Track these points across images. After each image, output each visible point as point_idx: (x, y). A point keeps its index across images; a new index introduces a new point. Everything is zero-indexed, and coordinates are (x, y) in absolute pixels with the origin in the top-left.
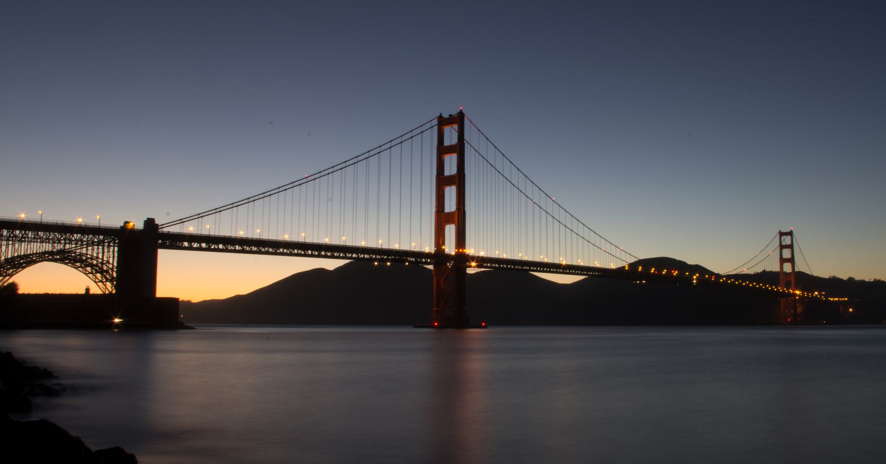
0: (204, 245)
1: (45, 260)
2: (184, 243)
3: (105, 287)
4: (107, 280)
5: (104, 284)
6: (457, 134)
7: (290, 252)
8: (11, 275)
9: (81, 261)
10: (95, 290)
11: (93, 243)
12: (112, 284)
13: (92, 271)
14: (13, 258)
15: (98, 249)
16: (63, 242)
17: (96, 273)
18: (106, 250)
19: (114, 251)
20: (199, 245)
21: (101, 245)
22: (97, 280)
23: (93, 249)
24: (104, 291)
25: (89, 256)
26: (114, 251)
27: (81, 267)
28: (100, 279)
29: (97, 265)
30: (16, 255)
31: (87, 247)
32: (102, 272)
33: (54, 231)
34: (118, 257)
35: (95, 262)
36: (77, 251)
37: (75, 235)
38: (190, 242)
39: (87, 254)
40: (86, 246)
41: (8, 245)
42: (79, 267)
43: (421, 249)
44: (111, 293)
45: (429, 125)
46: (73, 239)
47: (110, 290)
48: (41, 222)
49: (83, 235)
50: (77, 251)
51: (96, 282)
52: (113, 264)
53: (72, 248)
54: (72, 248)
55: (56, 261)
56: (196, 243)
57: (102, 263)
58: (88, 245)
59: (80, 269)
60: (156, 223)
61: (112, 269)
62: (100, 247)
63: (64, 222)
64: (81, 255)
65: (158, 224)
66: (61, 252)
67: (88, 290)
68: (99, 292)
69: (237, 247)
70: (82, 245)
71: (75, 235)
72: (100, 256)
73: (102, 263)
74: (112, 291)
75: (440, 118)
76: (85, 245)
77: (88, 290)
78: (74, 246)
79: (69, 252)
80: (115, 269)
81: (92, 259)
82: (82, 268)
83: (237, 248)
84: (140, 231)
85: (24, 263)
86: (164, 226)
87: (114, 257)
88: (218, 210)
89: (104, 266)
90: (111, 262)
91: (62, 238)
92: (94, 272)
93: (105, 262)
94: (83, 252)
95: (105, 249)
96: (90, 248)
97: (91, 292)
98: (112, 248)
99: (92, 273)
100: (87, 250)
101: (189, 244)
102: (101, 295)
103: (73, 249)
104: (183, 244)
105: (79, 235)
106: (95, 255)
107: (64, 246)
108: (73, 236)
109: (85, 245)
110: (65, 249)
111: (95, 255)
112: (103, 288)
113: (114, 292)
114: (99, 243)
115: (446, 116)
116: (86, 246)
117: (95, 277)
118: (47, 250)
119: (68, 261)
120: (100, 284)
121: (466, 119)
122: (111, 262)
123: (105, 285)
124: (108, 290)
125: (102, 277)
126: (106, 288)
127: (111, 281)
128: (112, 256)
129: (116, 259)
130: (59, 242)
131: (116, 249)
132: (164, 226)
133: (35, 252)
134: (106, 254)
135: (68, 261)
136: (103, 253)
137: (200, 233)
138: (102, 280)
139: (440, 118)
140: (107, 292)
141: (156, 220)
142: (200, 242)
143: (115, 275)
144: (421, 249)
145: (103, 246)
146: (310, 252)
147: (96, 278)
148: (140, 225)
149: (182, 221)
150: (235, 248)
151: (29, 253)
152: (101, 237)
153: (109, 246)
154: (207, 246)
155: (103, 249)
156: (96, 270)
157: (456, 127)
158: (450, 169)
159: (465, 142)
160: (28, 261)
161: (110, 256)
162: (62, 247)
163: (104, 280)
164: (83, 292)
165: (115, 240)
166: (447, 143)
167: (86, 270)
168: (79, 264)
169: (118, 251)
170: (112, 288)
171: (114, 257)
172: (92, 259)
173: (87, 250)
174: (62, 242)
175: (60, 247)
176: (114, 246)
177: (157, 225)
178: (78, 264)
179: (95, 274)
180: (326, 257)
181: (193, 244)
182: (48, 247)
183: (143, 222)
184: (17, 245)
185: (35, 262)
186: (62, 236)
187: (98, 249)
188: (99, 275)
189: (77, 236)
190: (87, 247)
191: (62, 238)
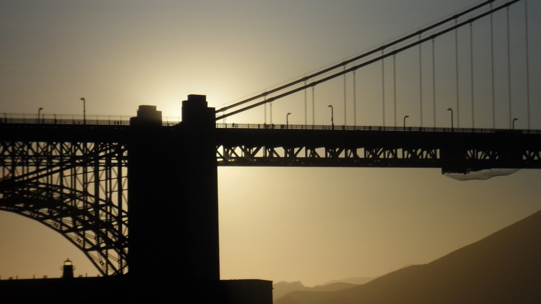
0: (321, 152)
2: (276, 149)
3: (104, 261)
4: (110, 245)
5: (102, 254)
7: (528, 157)
9: (51, 203)
12: (121, 253)
13: (75, 226)
15: (85, 172)
16: (8, 161)
17: (84, 229)
18: (103, 175)
19: (119, 177)
20: (309, 151)
21: (91, 165)
22: (88, 246)
23: (74, 175)
24: (104, 268)
25: (66, 191)
26: (119, 177)
27: (51, 217)
28: (94, 242)
29: (84, 211)
31: (61, 171)
34: (130, 189)
37: (34, 145)
39: (62, 187)
40: (58, 168)
42: (46, 217)
44: (118, 273)
46: (31, 153)
47: (117, 266)
49: (49, 142)
50: (41, 180)
51: (85, 251)
52: (120, 207)
53: (29, 174)
54: (29, 174)
56: (304, 149)
57: (97, 206)
58: (63, 166)
59: (50, 221)
60: (210, 105)
61: (119, 219)
62: (90, 169)
64: (50, 188)
67: (68, 270)
70: (50, 166)
71: (34, 145)
72: (91, 189)
73: (97, 206)
74: (122, 268)
76: (57, 165)
77: (68, 270)
78: (32, 169)
79: (23, 184)
81: (73, 197)
82: (54, 218)
83: (400, 155)
87: (120, 190)
88: (349, 66)
89: (101, 212)
90: (115, 201)
91: (7, 153)
92: (80, 227)
93: (101, 203)
94: (54, 183)
95: (100, 172)
96: (67, 172)
97: (76, 274)
98: (116, 168)
99: (74, 229)
100: (62, 176)
101: (286, 152)
102: (98, 278)
103: (31, 177)
104: (272, 151)
105: (42, 144)
106: (80, 188)
107: (12, 171)
108: (30, 147)
109: (57, 165)
110: (14, 177)
111: (80, 188)
113: (126, 271)
116: (58, 168)
117: (81, 239)
119: (21, 205)
120: (95, 254)
123: (106, 256)
125: (97, 238)
126: (108, 262)
127: (118, 247)
128: (116, 188)
129: (125, 193)
131: (125, 171)
134: (103, 184)
135: (21, 205)
136: (97, 182)
137: (310, 123)
138: (99, 244)
140: (111, 272)
141: (207, 100)
142: (312, 146)
143: (125, 231)
145: (96, 166)
147: (86, 240)
150: (395, 155)
152: (91, 146)
153: (109, 166)
154: (329, 154)
155: (96, 172)
156: (83, 222)
162: (7, 172)
163: (103, 245)
164: (58, 274)
165: (121, 152)
167: (63, 224)
168: (46, 209)
169: (129, 176)
171: (120, 190)
172: (73, 197)
173: (62, 176)
174: (6, 161)
176: (120, 166)
177: (213, 111)
179: (82, 233)
181: (296, 150)
183: (180, 106)
186: (5, 149)
187: (85, 172)
188: (90, 234)
189: (38, 145)
191: (7, 153)
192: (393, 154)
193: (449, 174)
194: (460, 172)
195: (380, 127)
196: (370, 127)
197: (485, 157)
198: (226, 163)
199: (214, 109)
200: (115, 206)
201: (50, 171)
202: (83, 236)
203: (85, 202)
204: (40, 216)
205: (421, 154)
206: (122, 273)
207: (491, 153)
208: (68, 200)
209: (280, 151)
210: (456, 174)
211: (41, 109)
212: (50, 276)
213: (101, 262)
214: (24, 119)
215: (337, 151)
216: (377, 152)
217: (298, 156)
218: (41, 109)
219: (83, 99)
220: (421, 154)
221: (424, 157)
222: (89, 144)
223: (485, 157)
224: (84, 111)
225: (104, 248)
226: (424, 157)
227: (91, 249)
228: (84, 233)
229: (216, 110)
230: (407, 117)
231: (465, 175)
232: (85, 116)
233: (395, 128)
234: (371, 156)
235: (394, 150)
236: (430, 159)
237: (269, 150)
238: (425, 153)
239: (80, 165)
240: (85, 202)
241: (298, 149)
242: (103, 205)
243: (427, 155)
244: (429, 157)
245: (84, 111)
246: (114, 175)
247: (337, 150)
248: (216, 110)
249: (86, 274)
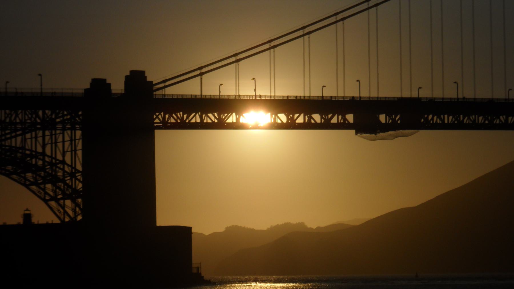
2: (279, 115)
3: (62, 211)
4: (66, 197)
5: (59, 205)
11: (32, 128)
15: (44, 136)
17: (45, 183)
18: (60, 139)
20: (340, 117)
22: (47, 198)
24: (62, 217)
26: (72, 140)
28: (51, 193)
29: (43, 168)
32: (54, 180)
34: (84, 149)
35: (40, 163)
36: (3, 143)
39: (23, 148)
43: (378, 94)
44: (73, 220)
47: (71, 213)
48: (42, 93)
51: (46, 201)
56: (302, 115)
59: (14, 176)
62: (47, 133)
63: (19, 91)
65: (151, 82)
67: (27, 217)
68: (57, 221)
72: (48, 151)
74: (76, 216)
77: (27, 217)
81: (31, 156)
84: (122, 94)
86: (167, 83)
90: (68, 159)
91: (58, 120)
94: (18, 145)
99: (35, 183)
100: (24, 140)
104: (310, 118)
111: (40, 149)
112: (60, 212)
120: (53, 203)
124: (69, 215)
125: (55, 192)
129: (80, 153)
131: (79, 133)
132: (167, 83)
134: (60, 145)
140: (67, 219)
141: (146, 74)
143: (80, 186)
144: (378, 94)
147: (46, 193)
163: (60, 197)
164: (21, 221)
167: (26, 179)
168: (10, 167)
170: (74, 211)
171: (74, 151)
178: (9, 168)
181: (296, 116)
183: (123, 79)
187: (44, 136)
191: (18, 121)
192: (441, 119)
193: (362, 135)
194: (371, 133)
195: (331, 97)
196: (288, 97)
197: (485, 121)
199: (152, 82)
200: (68, 165)
201: (13, 134)
202: (44, 190)
203: (44, 160)
204: (7, 172)
205: (432, 119)
206: (76, 219)
207: (489, 118)
208: (29, 159)
209: (317, 118)
210: (365, 135)
211: (7, 82)
212: (9, 223)
213: (58, 210)
214: (72, 93)
215: (330, 118)
216: (396, 117)
217: (297, 121)
218: (7, 82)
219: (40, 75)
220: (432, 119)
221: (434, 122)
222: (47, 111)
223: (485, 121)
224: (41, 85)
225: (61, 199)
226: (434, 122)
227: (51, 200)
228: (45, 187)
229: (154, 83)
230: (324, 86)
231: (376, 136)
232: (41, 89)
233: (378, 97)
234: (391, 121)
235: (442, 116)
236: (440, 123)
237: (307, 116)
238: (435, 118)
239: (39, 129)
240: (44, 160)
241: (297, 115)
242: (58, 164)
243: (437, 120)
244: (438, 122)
245: (41, 85)
246: (67, 138)
247: (330, 116)
248: (154, 83)
249: (52, 221)
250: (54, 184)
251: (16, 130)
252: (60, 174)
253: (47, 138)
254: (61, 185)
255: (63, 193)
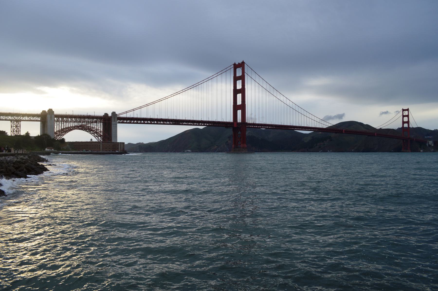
1: (75, 129)
4: (99, 136)
6: (245, 71)
8: (63, 135)
9: (89, 129)
10: (95, 140)
11: (93, 122)
14: (64, 129)
16: (98, 122)
17: (95, 133)
18: (98, 125)
26: (101, 125)
27: (89, 131)
29: (95, 130)
30: (65, 127)
31: (91, 124)
32: (97, 133)
33: (9, 116)
35: (94, 129)
37: (94, 119)
38: (150, 121)
41: (62, 124)
44: (101, 141)
45: (230, 68)
47: (100, 140)
49: (6, 116)
51: (95, 137)
55: (80, 129)
58: (91, 123)
62: (95, 123)
64: (88, 127)
66: (81, 126)
67: (91, 140)
69: (162, 122)
72: (96, 127)
75: (235, 64)
77: (91, 140)
80: (102, 132)
81: (92, 128)
85: (67, 130)
90: (100, 129)
99: (93, 133)
100: (91, 125)
111: (94, 127)
113: (102, 140)
114: (96, 122)
115: (237, 63)
118: (76, 125)
120: (96, 137)
121: (245, 65)
122: (100, 129)
129: (102, 128)
130: (80, 122)
131: (102, 124)
133: (71, 126)
134: (98, 126)
139: (235, 64)
142: (147, 121)
143: (102, 134)
146: (200, 124)
148: (110, 115)
149: (126, 112)
151: (69, 126)
157: (241, 68)
158: (239, 87)
159: (245, 74)
160: (69, 129)
161: (99, 127)
164: (89, 141)
166: (237, 75)
173: (91, 125)
175: (80, 124)
176: (101, 123)
177: (117, 114)
178: (88, 130)
180: (196, 125)
182: (76, 124)
184: (65, 124)
185: (72, 130)
188: (96, 134)
190: (91, 124)
198: (119, 123)
246: (100, 125)
250: (97, 134)
251: (89, 123)
252: (98, 132)
253: (95, 125)
254: (98, 134)
255: (99, 135)
